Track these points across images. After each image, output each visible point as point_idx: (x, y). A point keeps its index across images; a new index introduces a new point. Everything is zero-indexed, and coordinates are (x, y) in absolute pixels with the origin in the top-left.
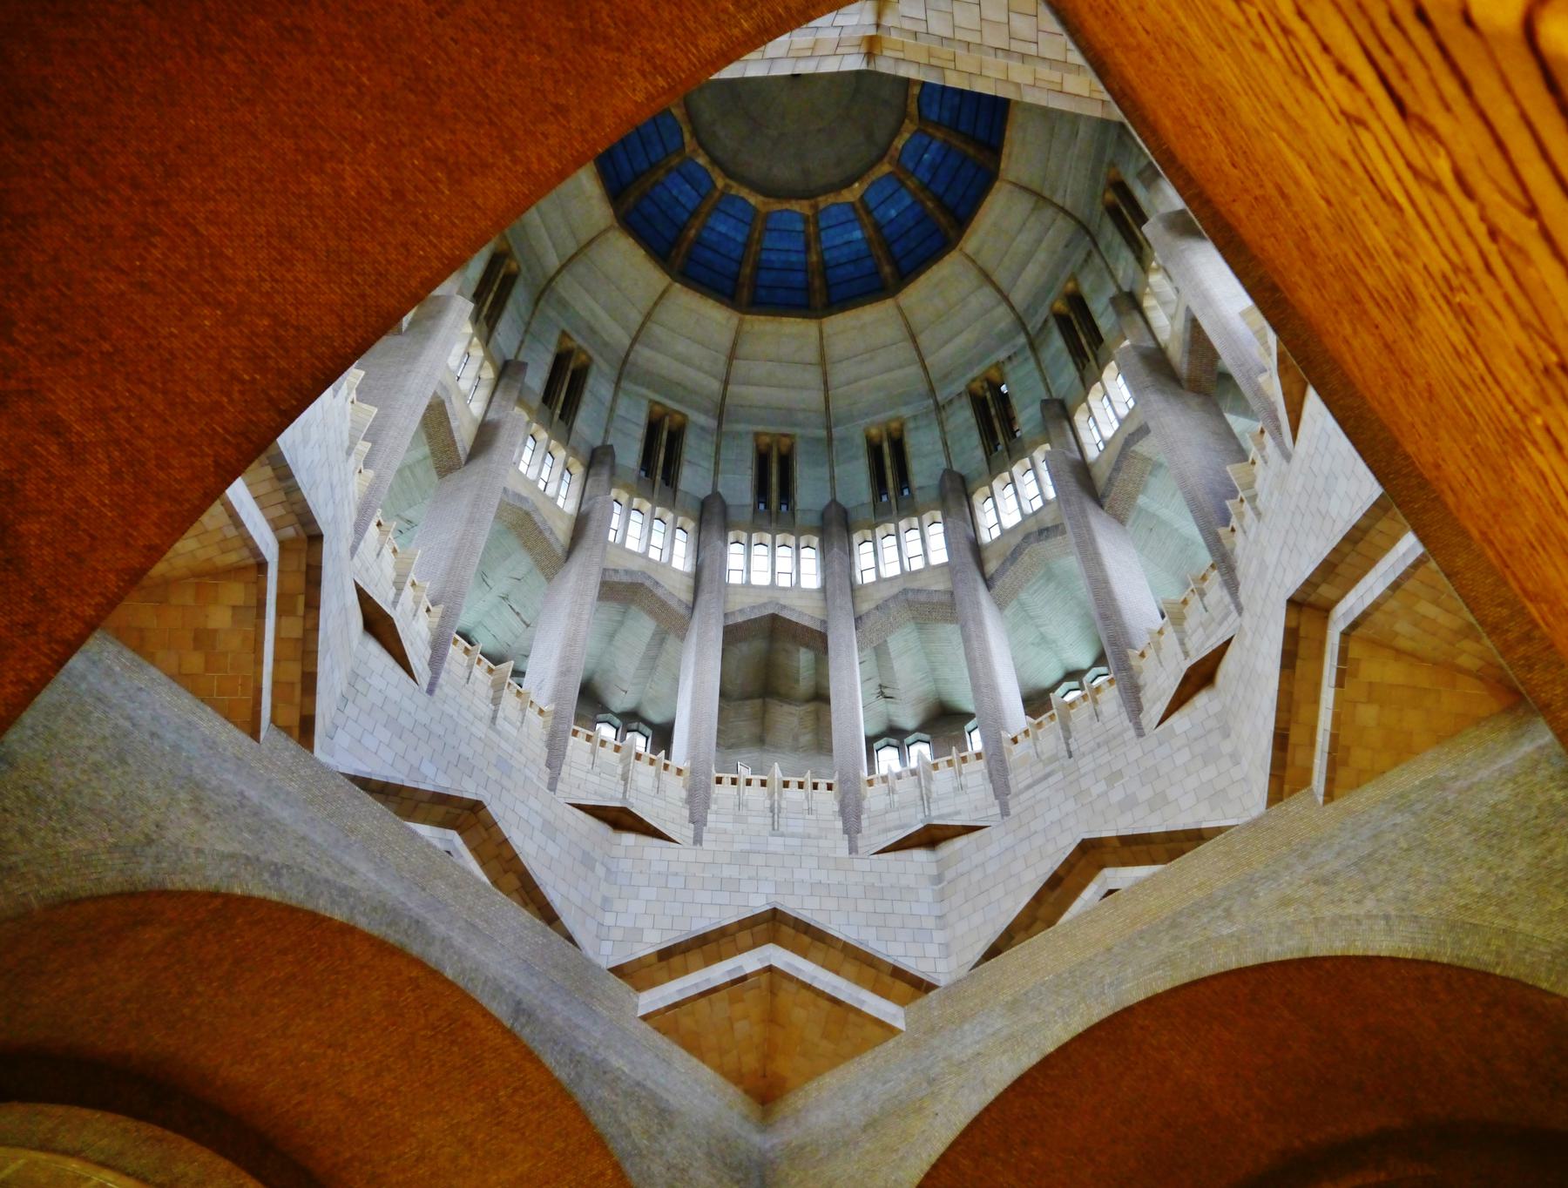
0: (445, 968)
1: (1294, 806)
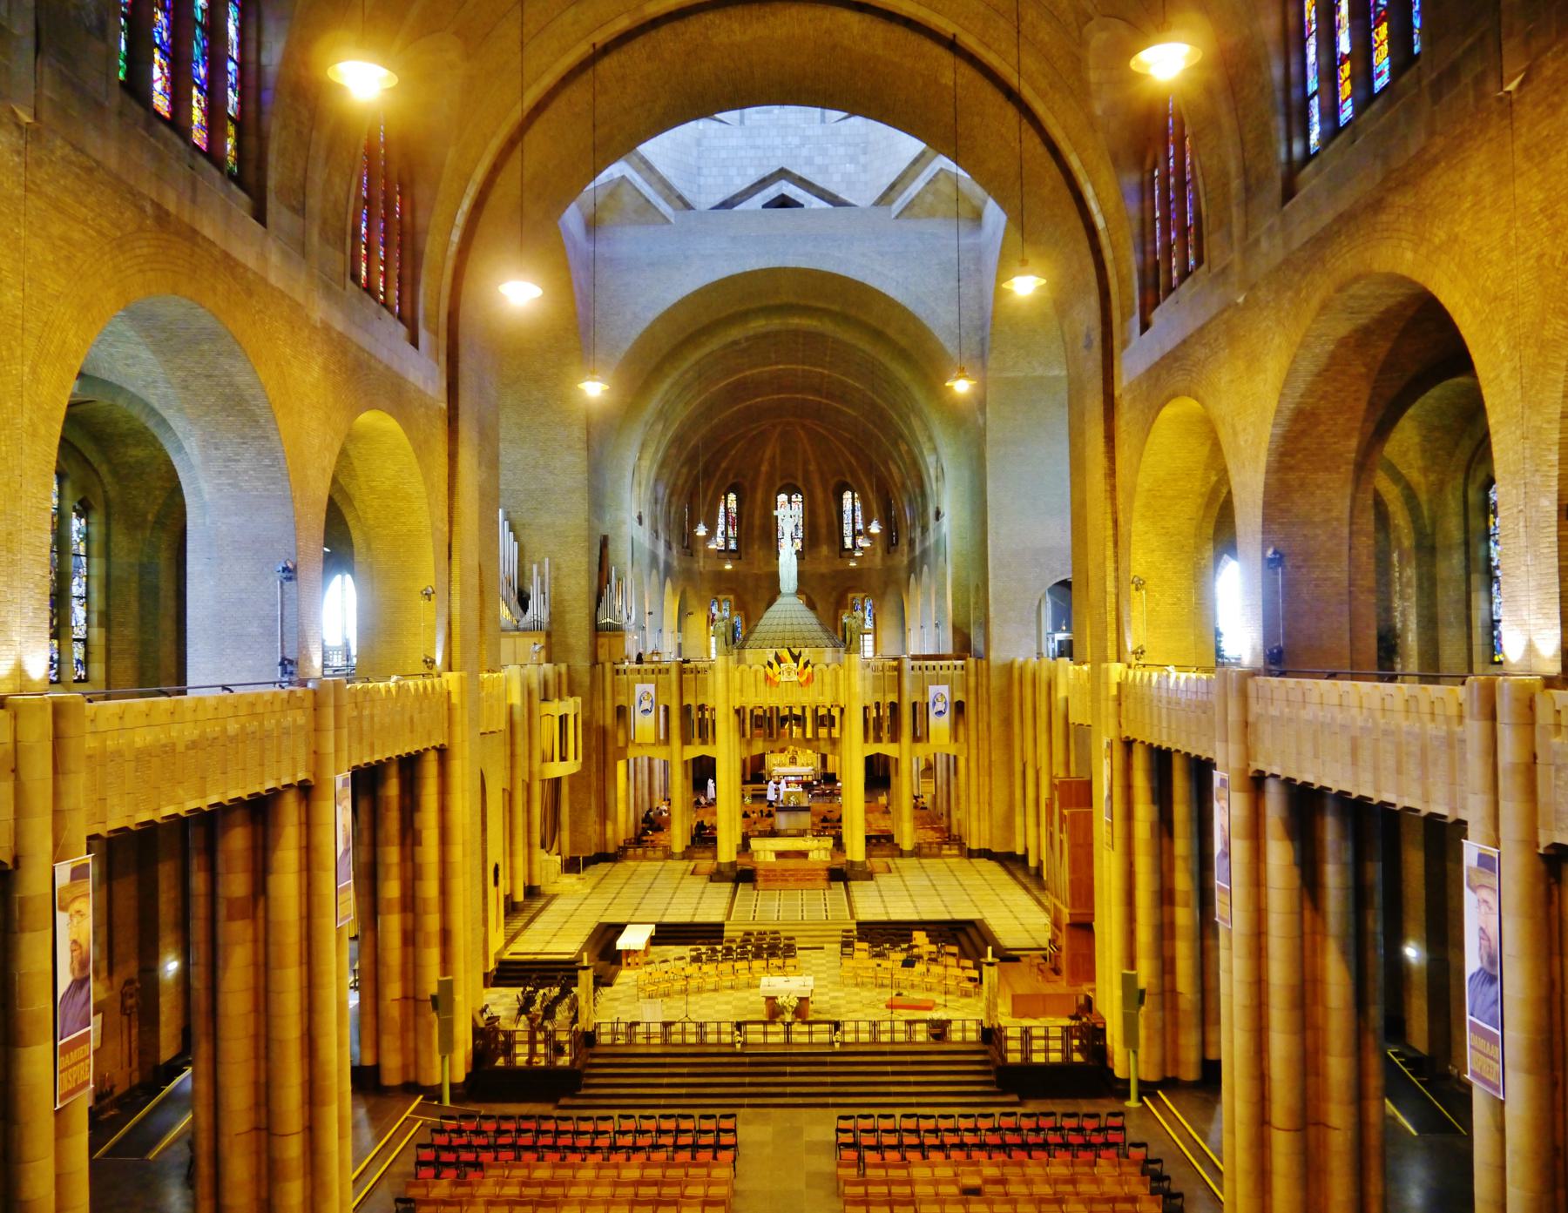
1: (882, 210)
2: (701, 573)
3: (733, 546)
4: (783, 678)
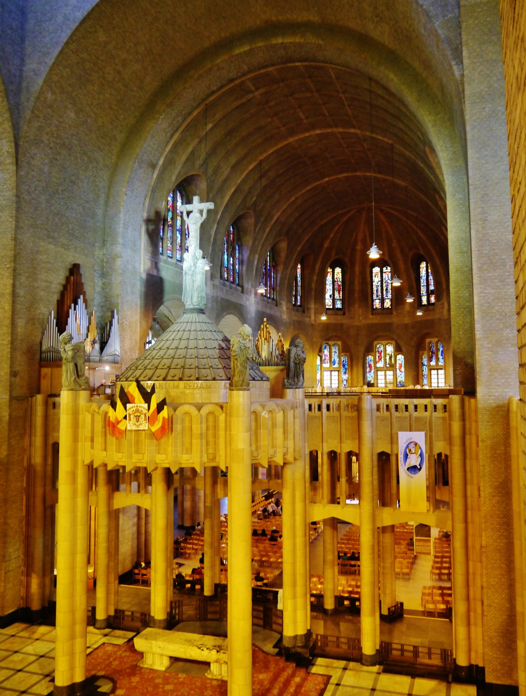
2: (312, 325)
3: (339, 305)
4: (130, 425)
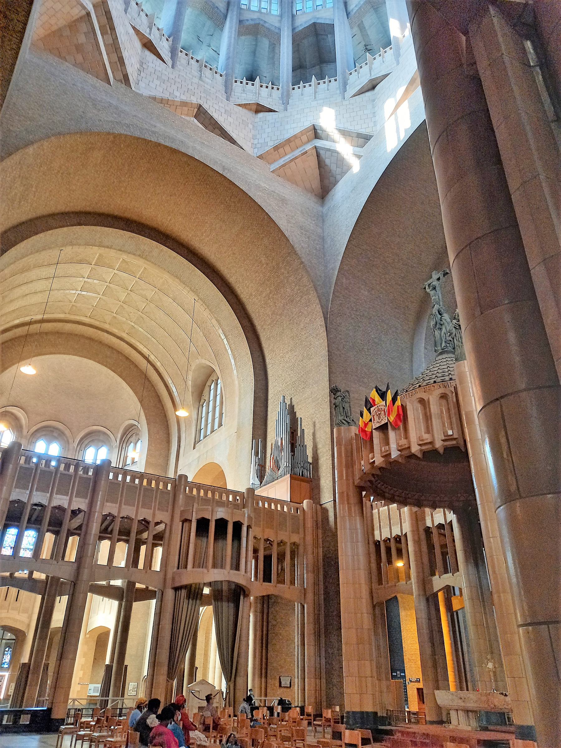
0: (195, 156)
